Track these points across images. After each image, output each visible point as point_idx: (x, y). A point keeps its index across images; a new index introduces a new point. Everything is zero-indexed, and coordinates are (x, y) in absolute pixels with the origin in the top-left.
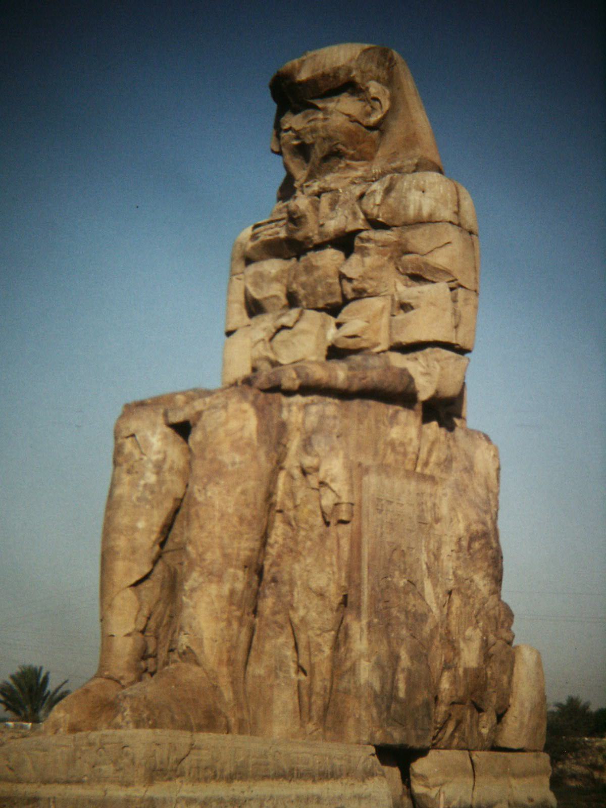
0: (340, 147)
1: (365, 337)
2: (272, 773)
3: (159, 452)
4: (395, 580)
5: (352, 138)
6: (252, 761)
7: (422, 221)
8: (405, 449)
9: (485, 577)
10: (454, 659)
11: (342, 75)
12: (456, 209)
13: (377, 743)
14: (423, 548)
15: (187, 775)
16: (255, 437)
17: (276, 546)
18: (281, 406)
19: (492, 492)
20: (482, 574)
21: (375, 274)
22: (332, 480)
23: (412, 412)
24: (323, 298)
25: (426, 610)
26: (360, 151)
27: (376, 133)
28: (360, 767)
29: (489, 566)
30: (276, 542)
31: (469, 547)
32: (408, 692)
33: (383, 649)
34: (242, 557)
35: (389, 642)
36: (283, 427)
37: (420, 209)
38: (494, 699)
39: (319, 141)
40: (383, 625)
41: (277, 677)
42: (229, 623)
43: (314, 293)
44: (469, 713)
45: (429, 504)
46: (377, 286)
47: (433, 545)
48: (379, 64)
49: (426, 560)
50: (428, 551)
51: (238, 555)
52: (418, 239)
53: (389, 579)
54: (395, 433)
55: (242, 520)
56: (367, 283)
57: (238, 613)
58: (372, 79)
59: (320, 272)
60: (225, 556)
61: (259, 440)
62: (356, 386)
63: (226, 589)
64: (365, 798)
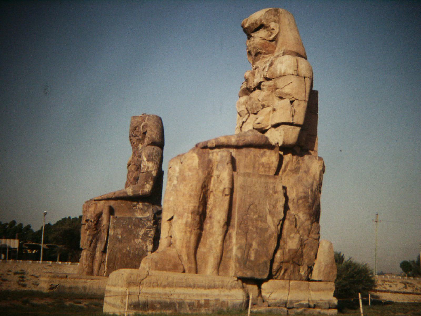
0: (259, 50)
1: (263, 123)
2: (184, 285)
6: (175, 281)
7: (281, 75)
10: (284, 245)
11: (259, 23)
12: (296, 69)
13: (238, 276)
14: (267, 204)
15: (145, 284)
16: (197, 166)
18: (209, 154)
19: (316, 180)
20: (302, 212)
23: (273, 151)
25: (267, 227)
26: (268, 51)
27: (274, 42)
28: (229, 284)
29: (306, 209)
31: (297, 202)
32: (255, 258)
33: (244, 241)
34: (190, 209)
35: (246, 239)
36: (210, 161)
38: (306, 261)
39: (252, 49)
40: (245, 232)
41: (210, 252)
42: (186, 233)
44: (292, 266)
45: (272, 187)
46: (268, 103)
47: (273, 202)
48: (275, 16)
50: (270, 204)
51: (189, 209)
52: (280, 83)
53: (248, 216)
54: (264, 160)
55: (190, 196)
56: (265, 102)
58: (272, 21)
60: (184, 209)
61: (199, 166)
62: (241, 143)
63: (184, 221)
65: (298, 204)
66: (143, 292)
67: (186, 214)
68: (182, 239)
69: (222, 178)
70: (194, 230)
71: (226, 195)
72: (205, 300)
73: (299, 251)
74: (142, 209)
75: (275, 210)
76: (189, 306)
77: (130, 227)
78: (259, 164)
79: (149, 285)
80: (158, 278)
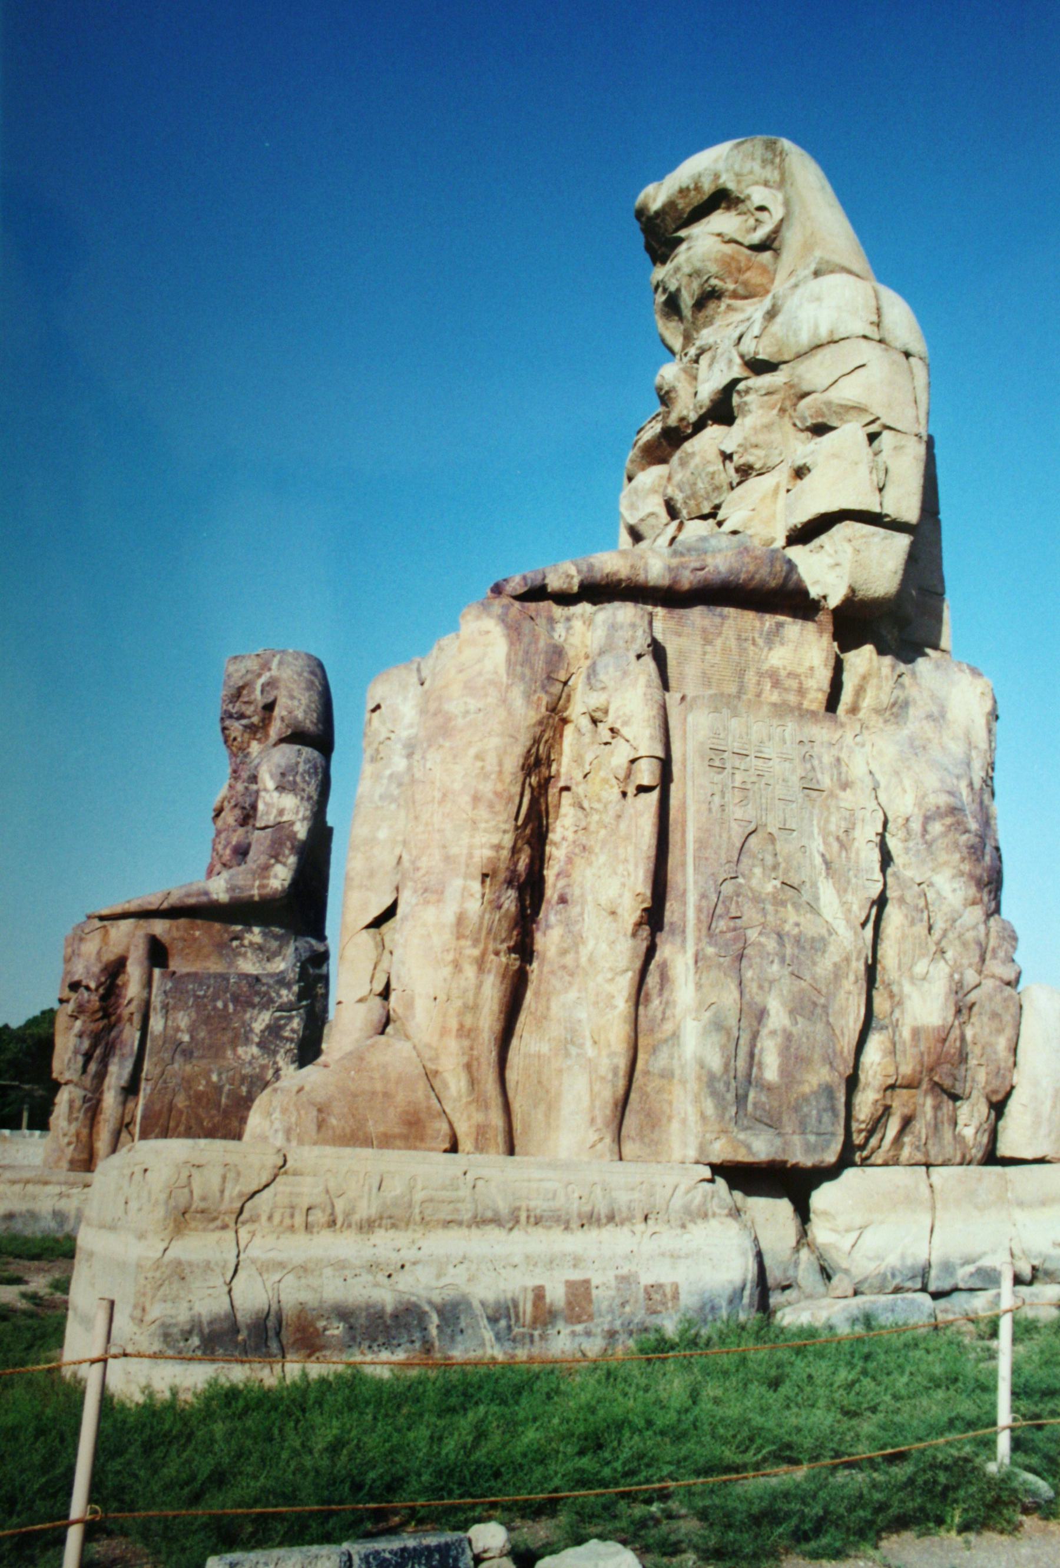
0: (714, 282)
1: (749, 532)
2: (467, 1216)
3: (411, 726)
4: (754, 883)
5: (730, 267)
6: (419, 1196)
8: (801, 683)
9: (954, 877)
10: (892, 1012)
11: (708, 187)
13: (716, 1160)
14: (816, 830)
15: (264, 1218)
16: (502, 670)
17: (565, 844)
18: (551, 621)
19: (976, 747)
20: (948, 872)
21: (761, 438)
22: (625, 723)
23: (810, 626)
24: (708, 498)
25: (824, 932)
26: (745, 284)
27: (767, 255)
28: (677, 1202)
29: (963, 860)
30: (564, 838)
31: (925, 831)
32: (785, 1071)
33: (729, 998)
34: (477, 859)
36: (557, 653)
37: (816, 327)
41: (567, 1055)
42: (457, 966)
43: (693, 495)
44: (929, 1102)
45: (827, 759)
46: (766, 456)
47: (836, 824)
48: (764, 162)
49: (822, 848)
50: (825, 834)
51: (470, 856)
52: (814, 373)
53: (741, 880)
54: (778, 657)
55: (476, 799)
56: (752, 454)
57: (476, 952)
58: (756, 183)
59: (697, 460)
60: (447, 859)
62: (687, 580)
64: (687, 1256)
65: (928, 837)
66: (253, 1262)
67: (458, 883)
68: (442, 997)
69: (618, 717)
70: (497, 953)
71: (642, 789)
72: (570, 1284)
73: (952, 1037)
74: (260, 948)
75: (848, 858)
76: (493, 1320)
77: (220, 1004)
78: (760, 675)
79: (287, 1221)
80: (332, 1185)
